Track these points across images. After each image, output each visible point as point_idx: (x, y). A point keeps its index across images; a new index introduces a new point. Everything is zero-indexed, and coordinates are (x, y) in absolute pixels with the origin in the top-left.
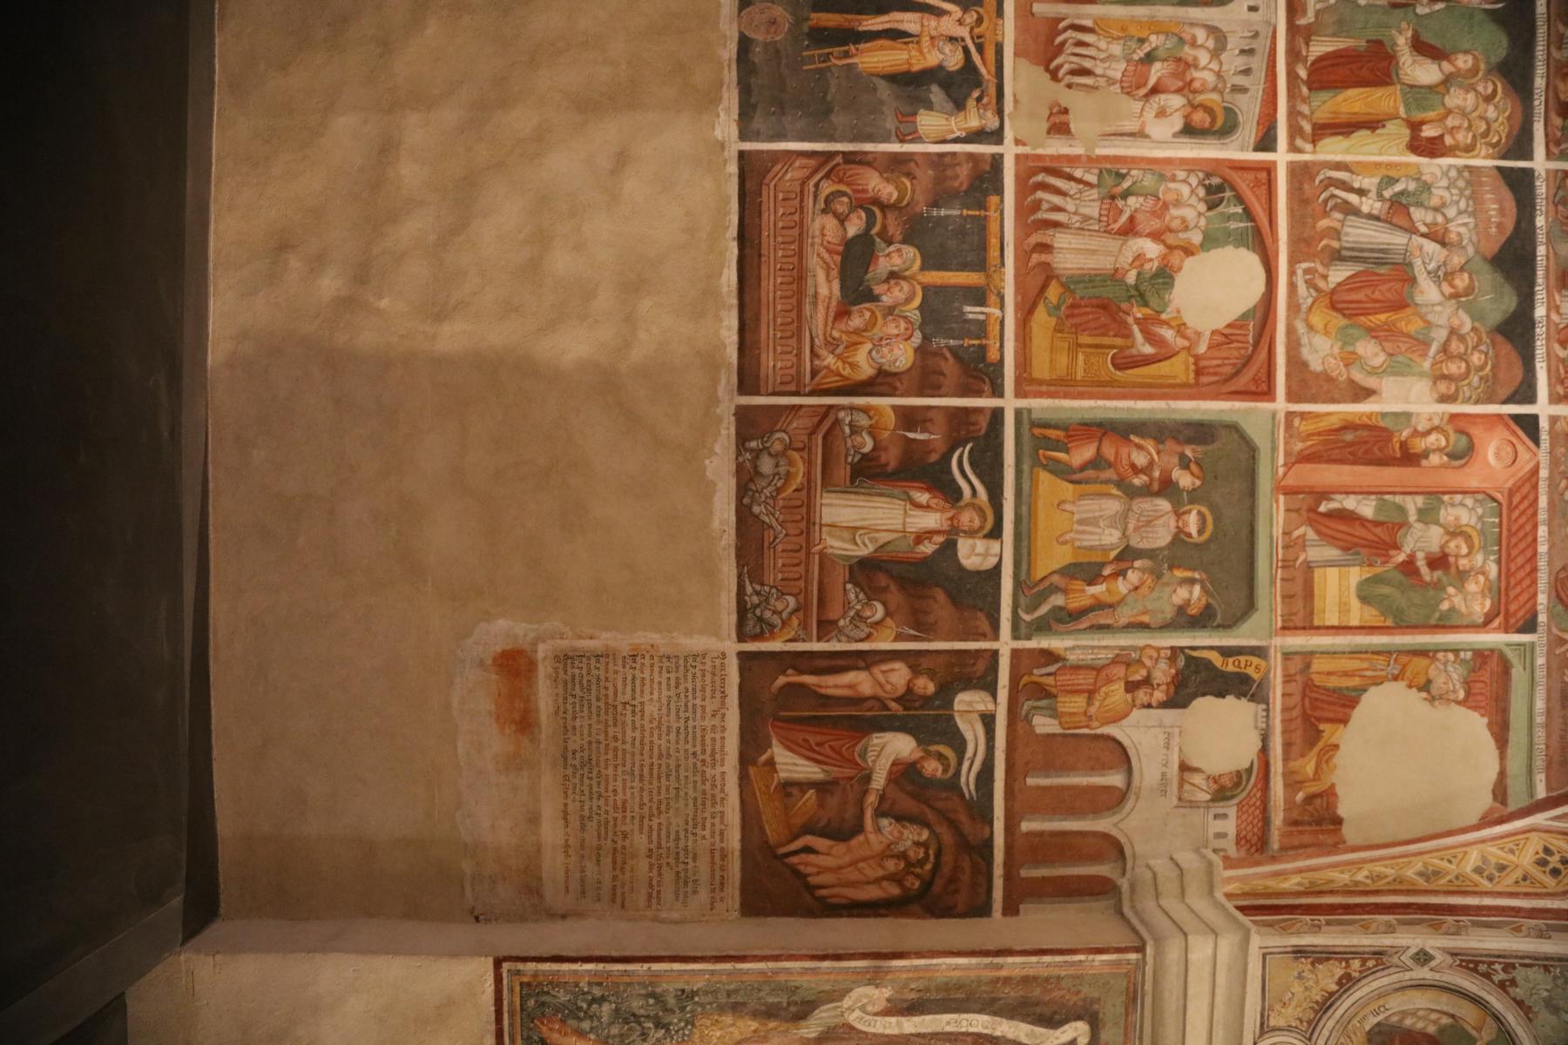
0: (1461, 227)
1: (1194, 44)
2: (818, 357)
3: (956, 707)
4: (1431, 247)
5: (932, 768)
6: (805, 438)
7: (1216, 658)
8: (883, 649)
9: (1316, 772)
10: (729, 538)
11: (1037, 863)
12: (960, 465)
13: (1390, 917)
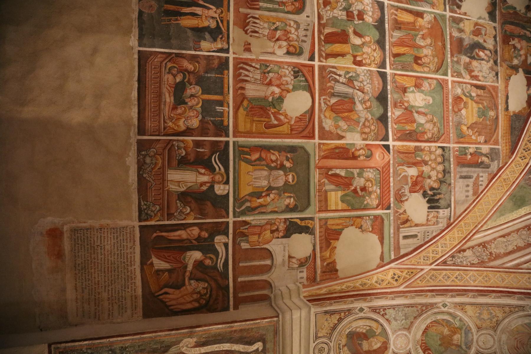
2: (166, 123)
3: (215, 241)
4: (360, 93)
5: (208, 262)
6: (162, 151)
7: (299, 222)
8: (190, 222)
9: (330, 256)
10: (135, 185)
11: (244, 292)
12: (215, 160)
13: (352, 299)
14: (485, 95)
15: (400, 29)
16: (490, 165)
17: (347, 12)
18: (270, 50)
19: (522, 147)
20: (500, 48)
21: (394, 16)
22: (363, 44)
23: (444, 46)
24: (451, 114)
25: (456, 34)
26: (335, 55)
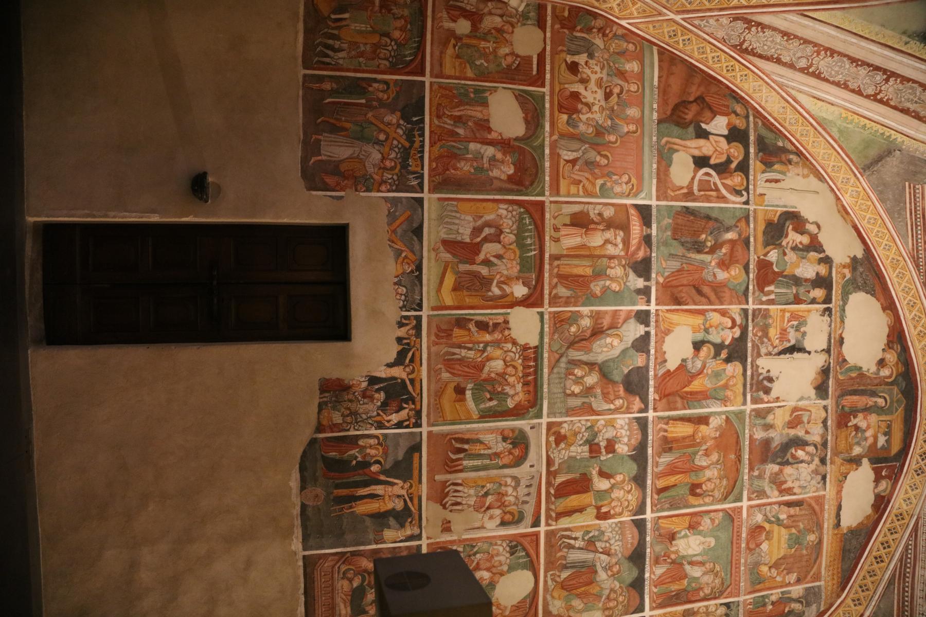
0: (616, 546)
1: (506, 485)
4: (603, 557)
14: (803, 512)
15: (670, 449)
16: (804, 612)
17: (590, 446)
18: (477, 525)
19: (859, 582)
20: (833, 435)
21: (662, 433)
22: (613, 487)
23: (739, 459)
24: (743, 555)
25: (760, 435)
26: (569, 513)
